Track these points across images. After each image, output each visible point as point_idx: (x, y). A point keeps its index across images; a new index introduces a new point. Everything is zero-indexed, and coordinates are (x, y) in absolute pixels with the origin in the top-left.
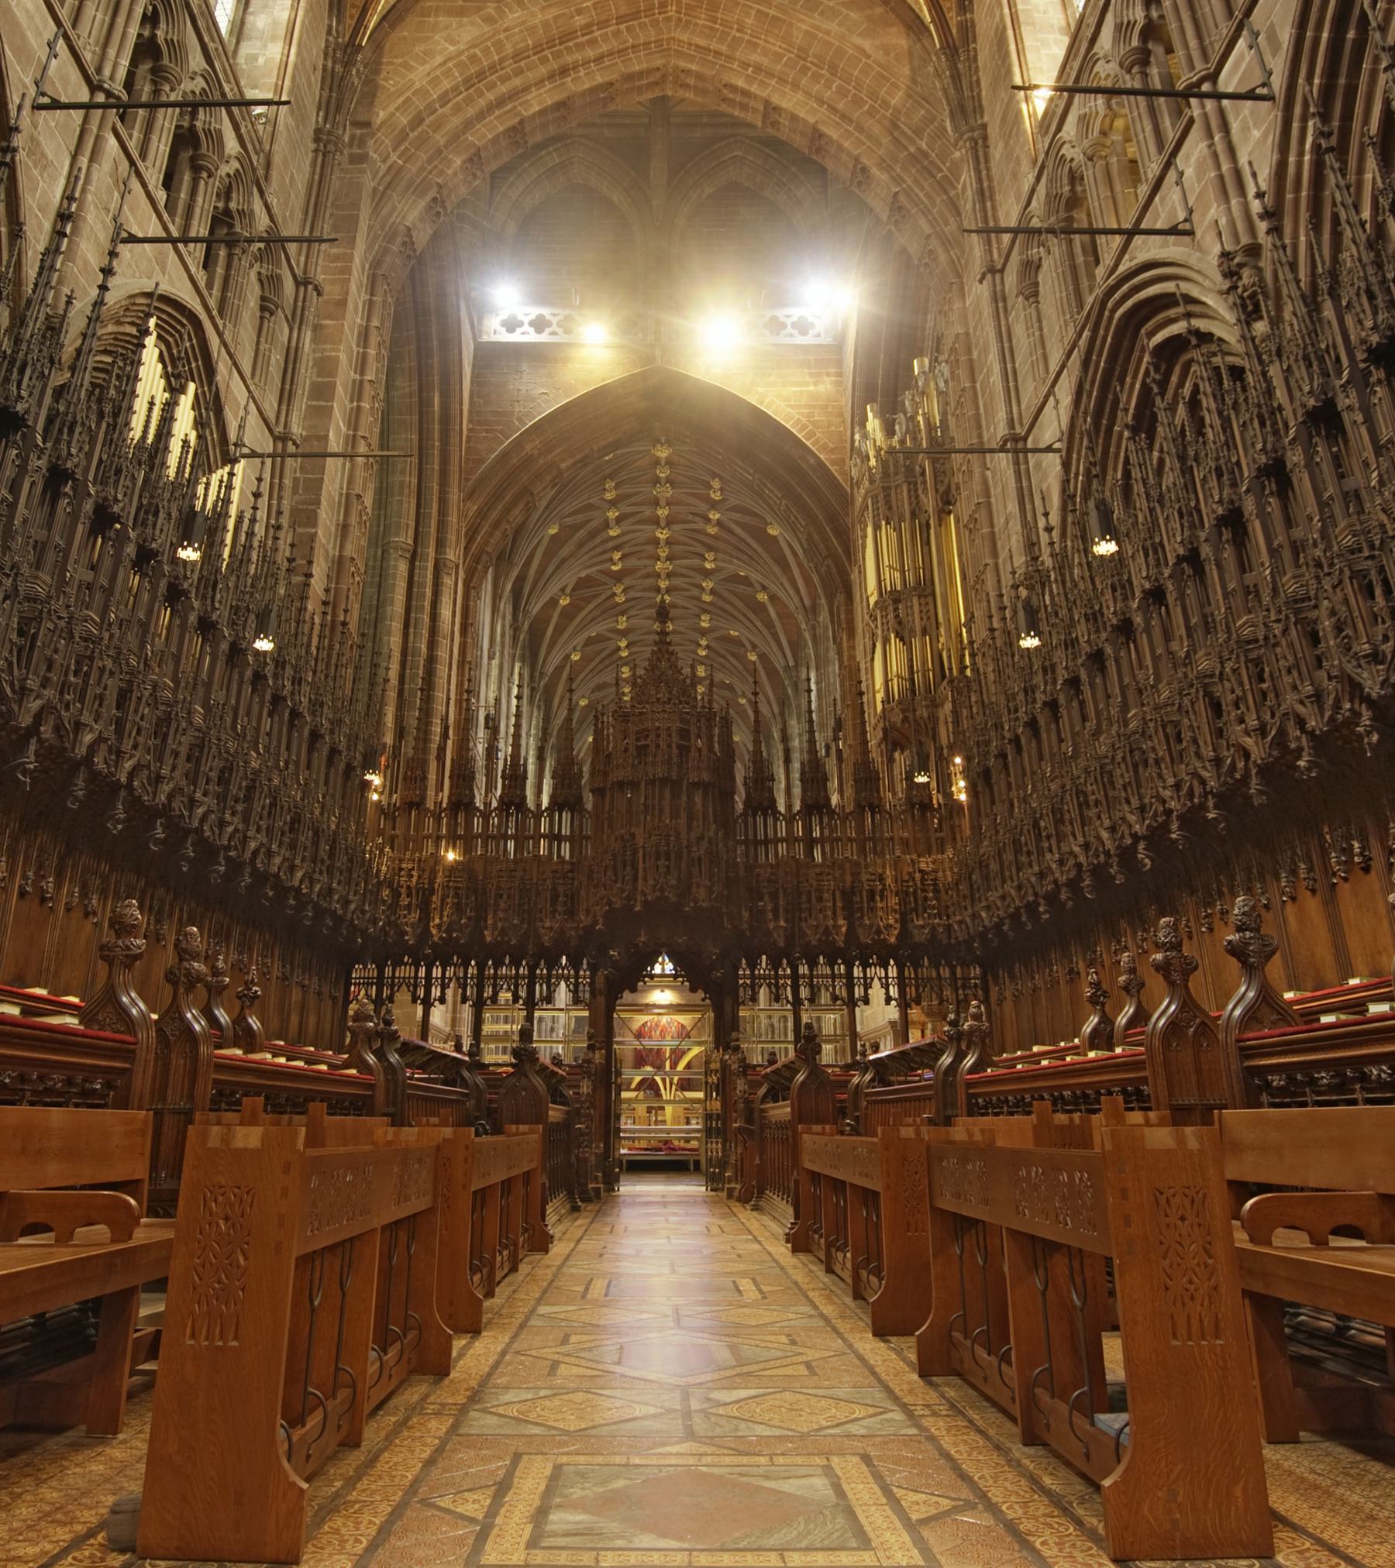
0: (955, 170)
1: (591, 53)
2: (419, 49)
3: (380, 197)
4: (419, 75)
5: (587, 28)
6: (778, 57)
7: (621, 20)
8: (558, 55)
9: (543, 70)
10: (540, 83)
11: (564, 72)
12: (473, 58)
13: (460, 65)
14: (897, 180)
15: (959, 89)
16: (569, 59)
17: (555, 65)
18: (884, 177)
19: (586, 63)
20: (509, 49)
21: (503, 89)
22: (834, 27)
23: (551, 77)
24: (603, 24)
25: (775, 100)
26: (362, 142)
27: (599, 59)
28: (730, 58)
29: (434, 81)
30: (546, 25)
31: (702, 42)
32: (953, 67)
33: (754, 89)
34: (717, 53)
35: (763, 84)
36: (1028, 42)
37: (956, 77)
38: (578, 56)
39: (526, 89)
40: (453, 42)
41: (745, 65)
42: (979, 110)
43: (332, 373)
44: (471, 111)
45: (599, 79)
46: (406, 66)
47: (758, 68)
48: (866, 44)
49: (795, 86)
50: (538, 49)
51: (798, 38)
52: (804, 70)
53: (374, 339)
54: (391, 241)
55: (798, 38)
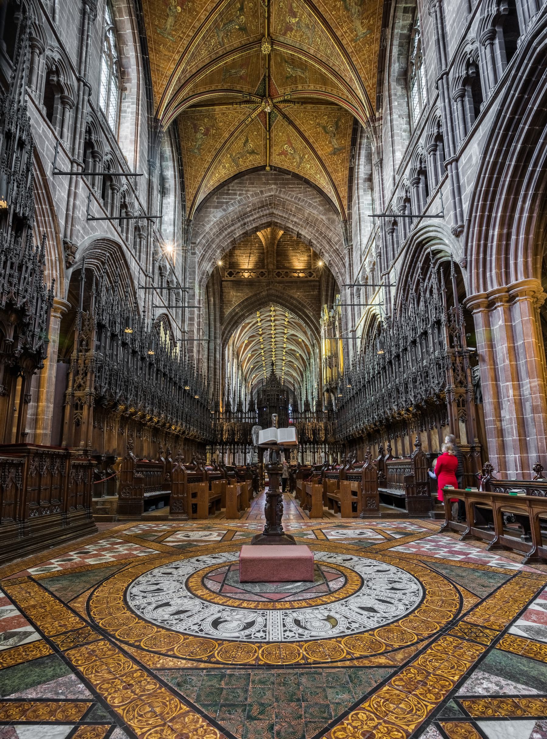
0: (345, 254)
1: (251, 218)
2: (206, 219)
3: (200, 264)
4: (207, 229)
5: (250, 211)
6: (301, 219)
7: (259, 208)
8: (243, 219)
9: (239, 224)
10: (238, 228)
11: (245, 224)
12: (221, 222)
13: (218, 224)
14: (330, 256)
15: (347, 233)
16: (246, 220)
17: (242, 222)
18: (327, 255)
19: (250, 221)
20: (230, 219)
21: (229, 230)
22: (315, 212)
23: (241, 226)
24: (255, 210)
25: (300, 232)
26: (194, 249)
27: (254, 220)
28: (288, 219)
29: (211, 229)
30: (239, 211)
31: (281, 214)
32: (346, 227)
33: (295, 228)
34: (285, 218)
35: (297, 227)
36: (362, 227)
37: (346, 230)
38: (248, 220)
39: (235, 230)
40: (215, 218)
41: (292, 221)
42: (351, 240)
43: (193, 314)
44: (221, 237)
45: (254, 226)
46: (203, 225)
47: (296, 222)
48: (324, 218)
49: (305, 228)
50: (238, 218)
51: (306, 215)
52: (308, 223)
53: (201, 303)
54: (203, 275)
55: (306, 215)
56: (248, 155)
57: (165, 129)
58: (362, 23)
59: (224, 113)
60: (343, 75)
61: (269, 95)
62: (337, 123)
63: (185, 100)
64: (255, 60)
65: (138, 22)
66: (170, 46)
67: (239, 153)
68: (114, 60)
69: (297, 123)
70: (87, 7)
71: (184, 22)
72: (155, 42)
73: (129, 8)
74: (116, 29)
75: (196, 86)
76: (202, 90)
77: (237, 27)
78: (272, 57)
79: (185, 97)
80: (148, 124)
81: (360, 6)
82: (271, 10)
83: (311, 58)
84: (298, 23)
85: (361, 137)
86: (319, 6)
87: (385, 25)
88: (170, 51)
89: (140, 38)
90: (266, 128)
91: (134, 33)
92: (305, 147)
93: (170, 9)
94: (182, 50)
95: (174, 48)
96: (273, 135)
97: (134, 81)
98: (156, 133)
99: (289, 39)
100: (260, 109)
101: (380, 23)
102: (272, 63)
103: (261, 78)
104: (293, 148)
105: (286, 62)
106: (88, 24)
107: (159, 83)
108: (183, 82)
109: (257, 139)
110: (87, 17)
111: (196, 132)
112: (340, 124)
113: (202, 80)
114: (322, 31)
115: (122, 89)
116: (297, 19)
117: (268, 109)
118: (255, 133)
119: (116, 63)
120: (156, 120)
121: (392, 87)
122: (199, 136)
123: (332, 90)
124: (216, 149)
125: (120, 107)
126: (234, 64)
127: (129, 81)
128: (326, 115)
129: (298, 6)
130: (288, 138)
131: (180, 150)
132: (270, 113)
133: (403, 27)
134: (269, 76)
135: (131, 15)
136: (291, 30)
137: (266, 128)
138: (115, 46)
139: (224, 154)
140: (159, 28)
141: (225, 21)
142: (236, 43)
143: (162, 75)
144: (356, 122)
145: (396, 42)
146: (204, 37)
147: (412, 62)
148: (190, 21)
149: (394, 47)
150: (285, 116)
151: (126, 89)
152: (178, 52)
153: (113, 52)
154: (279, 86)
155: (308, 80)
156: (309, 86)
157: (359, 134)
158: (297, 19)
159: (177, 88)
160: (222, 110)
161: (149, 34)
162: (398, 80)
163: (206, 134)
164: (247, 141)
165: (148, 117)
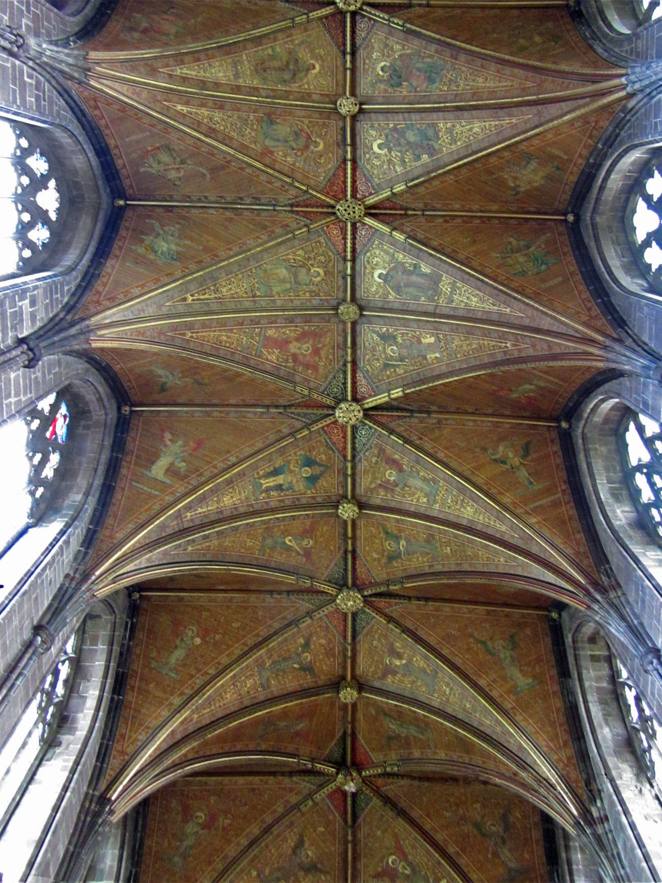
56: (301, 874)
57: (116, 818)
58: (521, 671)
59: (253, 790)
60: (502, 741)
61: (354, 763)
62: (504, 818)
63: (175, 766)
64: (326, 710)
65: (121, 654)
66: (169, 686)
67: (279, 869)
68: (56, 700)
69: (416, 813)
70: (39, 639)
71: (202, 656)
72: (141, 679)
73: (112, 638)
74: (78, 665)
75: (205, 744)
76: (214, 751)
77: (296, 666)
78: (360, 707)
79: (177, 762)
80: (83, 806)
81: (512, 650)
82: (358, 648)
83: (435, 714)
84: (405, 665)
85: (567, 848)
86: (441, 648)
87: (564, 673)
88: (165, 692)
89: (117, 674)
90: (345, 821)
91: (107, 668)
92: (439, 863)
93: (182, 640)
94: (188, 692)
95: (174, 688)
96: (361, 835)
97: (81, 733)
98: (93, 824)
99: (390, 683)
100: (332, 786)
101: (554, 672)
102: (360, 715)
103: (338, 735)
104: (410, 864)
105: (386, 714)
106: (30, 659)
107: (130, 737)
108: (179, 737)
109: (324, 841)
110: (31, 651)
111: (185, 821)
112: (511, 819)
113: (218, 736)
114: (451, 678)
115: (50, 744)
116: (404, 662)
117: (351, 787)
118: (322, 829)
119: (56, 705)
120: (104, 800)
121: (611, 765)
122: (191, 828)
123: (483, 762)
124: (226, 857)
125: (34, 774)
126: (285, 714)
127: (72, 731)
128: (477, 801)
129: (403, 647)
130: (397, 841)
131: (140, 855)
132: (354, 795)
133: (599, 679)
134: (354, 735)
135: (111, 644)
136: (394, 673)
137: (345, 821)
138: (66, 682)
139: (242, 871)
140: (157, 661)
141: (275, 657)
142: (291, 684)
143: (141, 725)
144: (547, 819)
145: (592, 698)
146: (234, 676)
147: (634, 728)
148: (213, 655)
149: (590, 705)
150: (387, 800)
151: (59, 744)
152: (182, 694)
153: (60, 690)
154: (373, 750)
155: (432, 744)
156: (435, 753)
157: (561, 843)
158: (404, 662)
159: (164, 747)
160: (251, 783)
161: (135, 668)
162: (617, 753)
163: (206, 826)
164: (300, 844)
165: (87, 794)
